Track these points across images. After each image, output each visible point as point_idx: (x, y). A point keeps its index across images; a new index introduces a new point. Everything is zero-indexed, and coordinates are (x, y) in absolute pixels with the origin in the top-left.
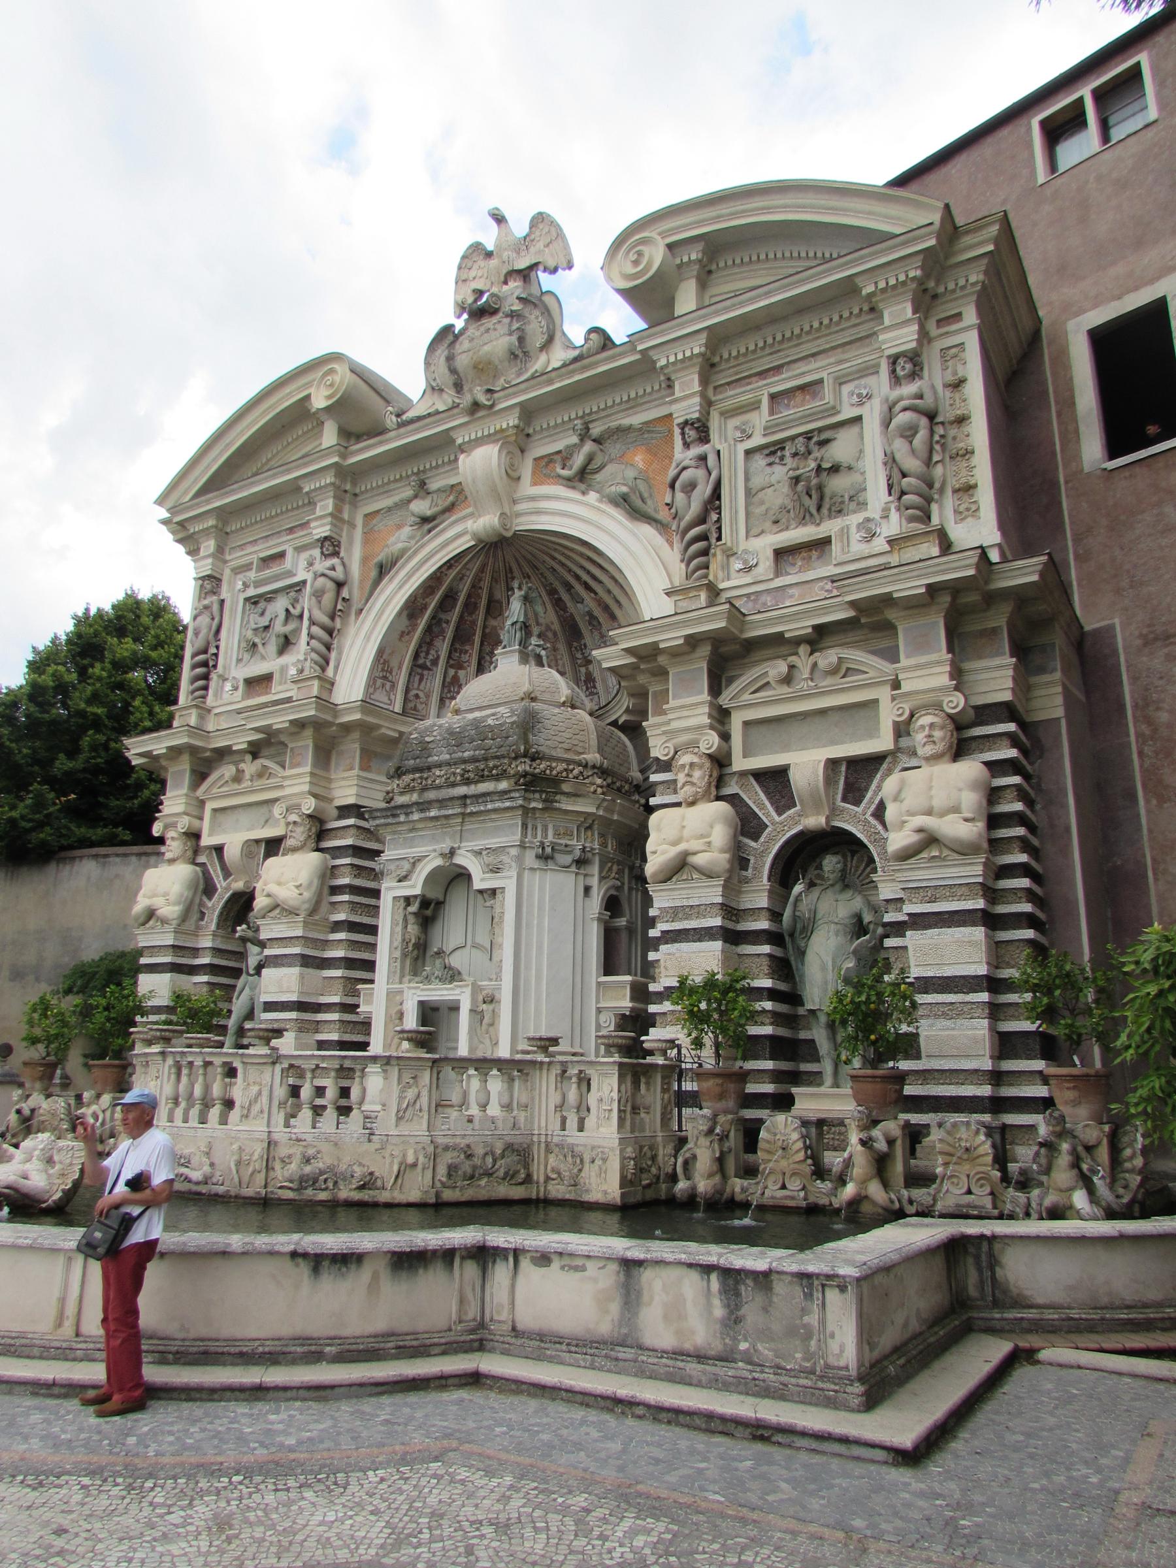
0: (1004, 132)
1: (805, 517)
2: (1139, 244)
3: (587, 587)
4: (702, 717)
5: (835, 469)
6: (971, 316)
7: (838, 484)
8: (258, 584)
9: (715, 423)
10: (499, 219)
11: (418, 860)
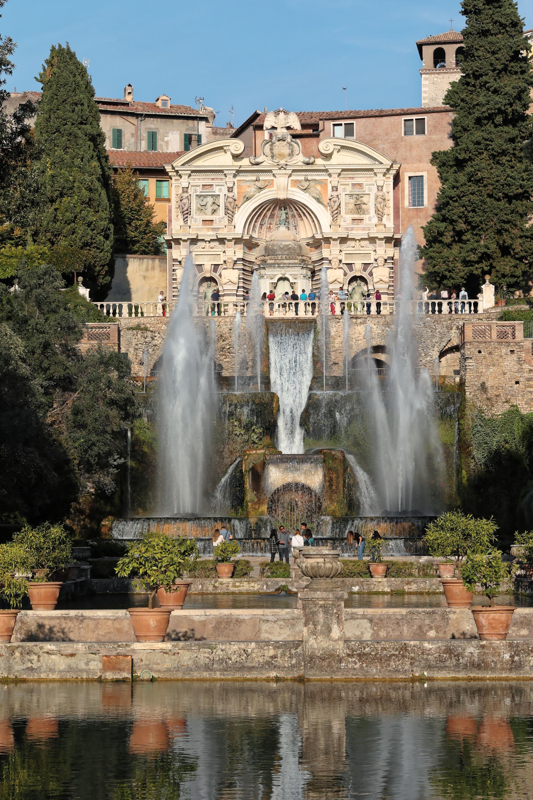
0: (396, 117)
2: (420, 161)
3: (296, 209)
5: (364, 204)
7: (364, 206)
8: (201, 192)
11: (276, 275)
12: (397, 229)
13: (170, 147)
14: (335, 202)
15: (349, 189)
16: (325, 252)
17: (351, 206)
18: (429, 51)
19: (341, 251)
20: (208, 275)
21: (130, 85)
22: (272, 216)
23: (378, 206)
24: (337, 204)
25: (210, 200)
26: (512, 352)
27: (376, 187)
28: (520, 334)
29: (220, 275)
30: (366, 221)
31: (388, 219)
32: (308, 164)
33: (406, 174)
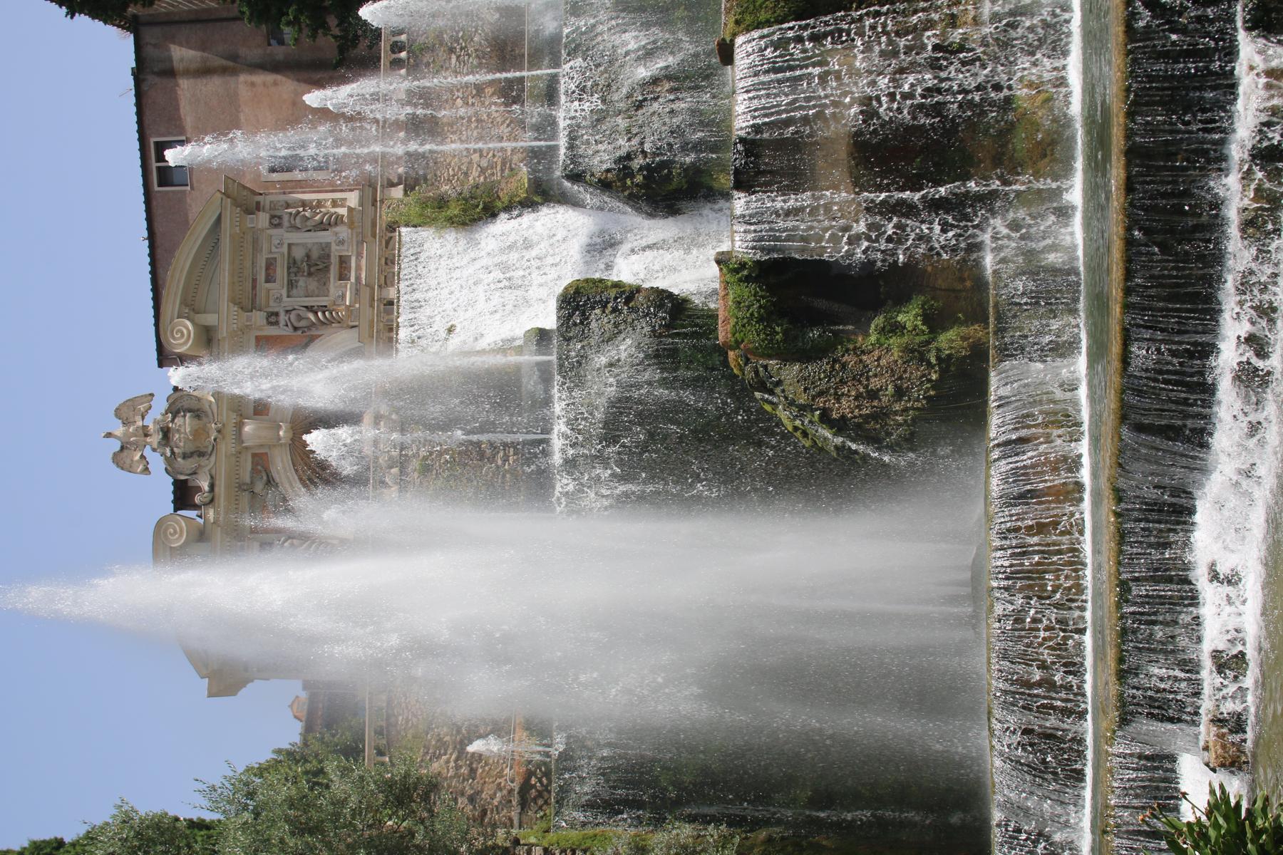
0: (154, 203)
1: (327, 269)
5: (308, 256)
7: (315, 255)
9: (271, 310)
10: (109, 435)
17: (313, 284)
27: (274, 231)
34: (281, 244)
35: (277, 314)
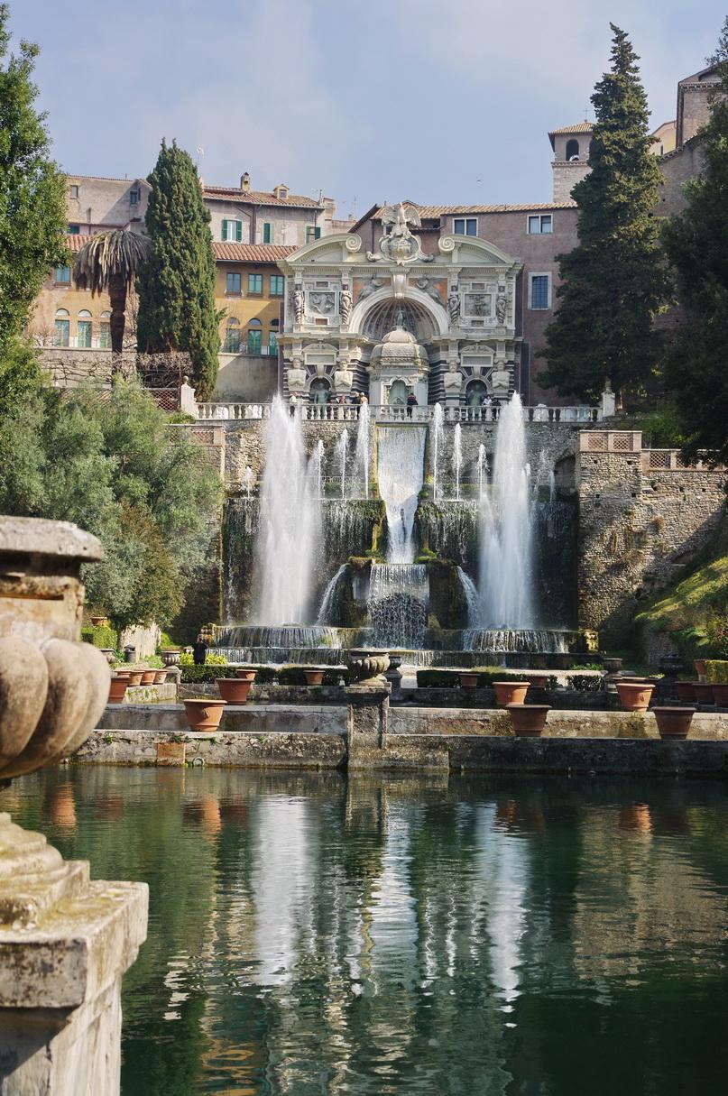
1: (478, 314)
2: (545, 261)
4: (456, 355)
5: (485, 305)
6: (514, 279)
7: (485, 308)
12: (518, 333)
13: (287, 241)
14: (454, 302)
15: (469, 290)
16: (442, 356)
18: (562, 145)
19: (459, 354)
20: (321, 377)
21: (246, 174)
22: (389, 316)
23: (500, 306)
24: (457, 304)
25: (323, 297)
26: (629, 463)
27: (497, 288)
28: (637, 446)
29: (333, 377)
30: (487, 324)
31: (510, 322)
32: (427, 261)
33: (530, 273)
34: (491, 290)
35: (457, 290)
